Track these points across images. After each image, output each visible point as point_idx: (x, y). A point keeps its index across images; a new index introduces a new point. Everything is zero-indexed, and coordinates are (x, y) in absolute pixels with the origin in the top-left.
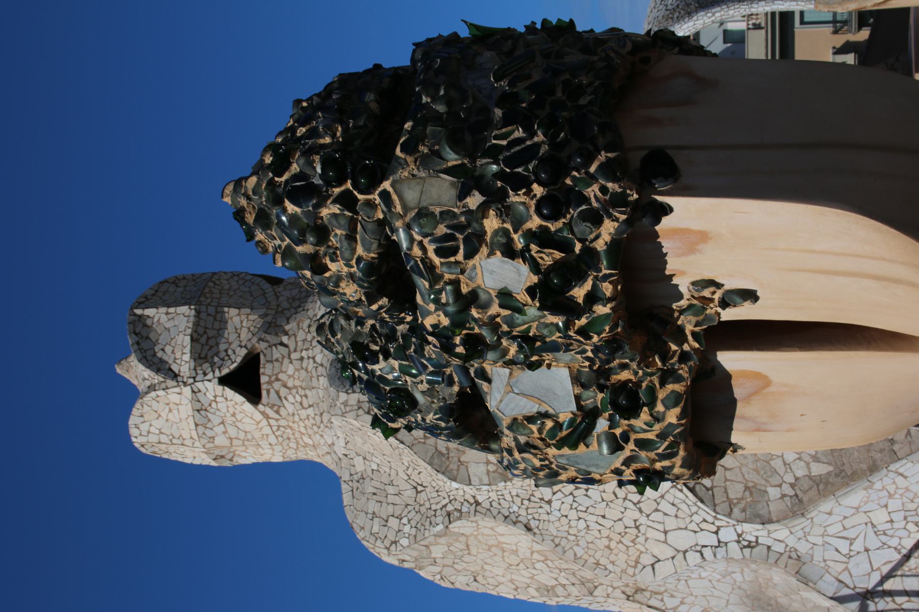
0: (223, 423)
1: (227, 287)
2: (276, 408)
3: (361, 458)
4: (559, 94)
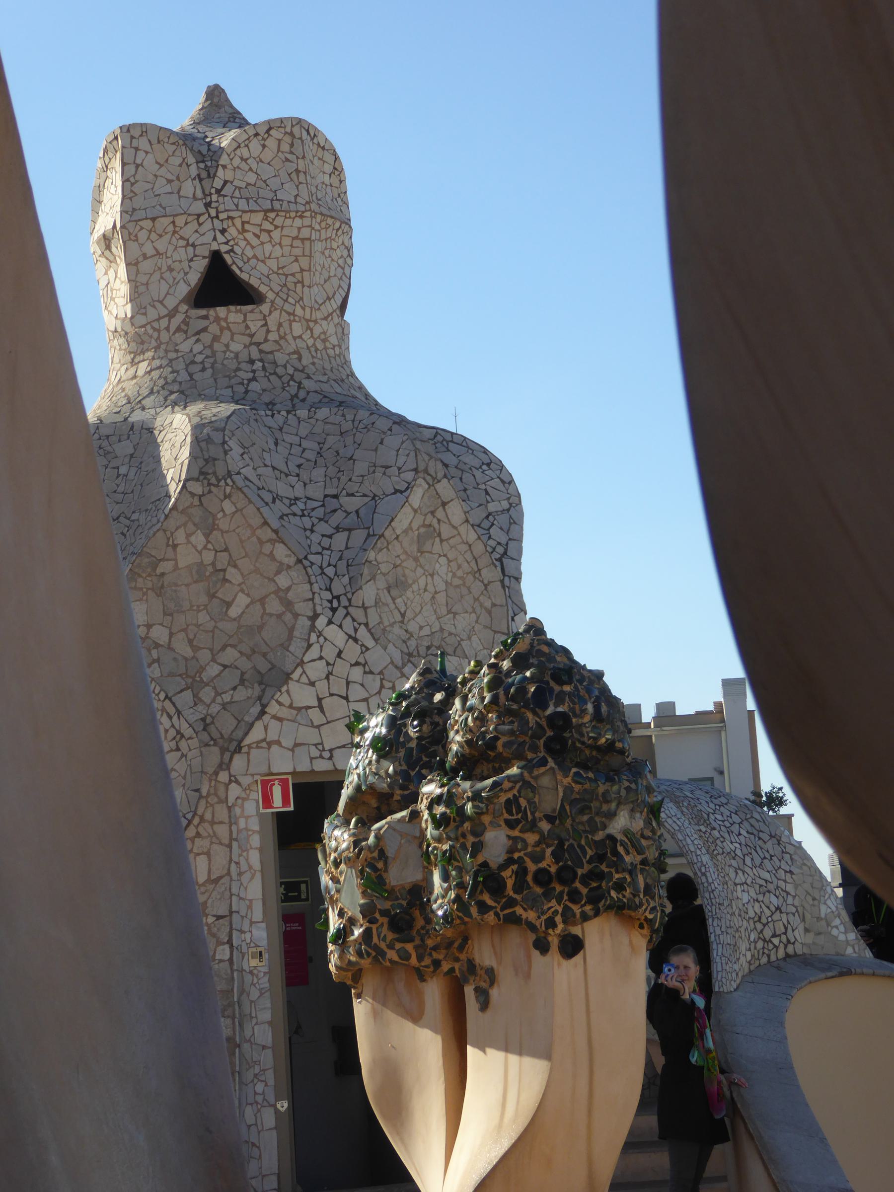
0: (158, 253)
1: (334, 245)
2: (184, 327)
3: (131, 451)
4: (617, 876)
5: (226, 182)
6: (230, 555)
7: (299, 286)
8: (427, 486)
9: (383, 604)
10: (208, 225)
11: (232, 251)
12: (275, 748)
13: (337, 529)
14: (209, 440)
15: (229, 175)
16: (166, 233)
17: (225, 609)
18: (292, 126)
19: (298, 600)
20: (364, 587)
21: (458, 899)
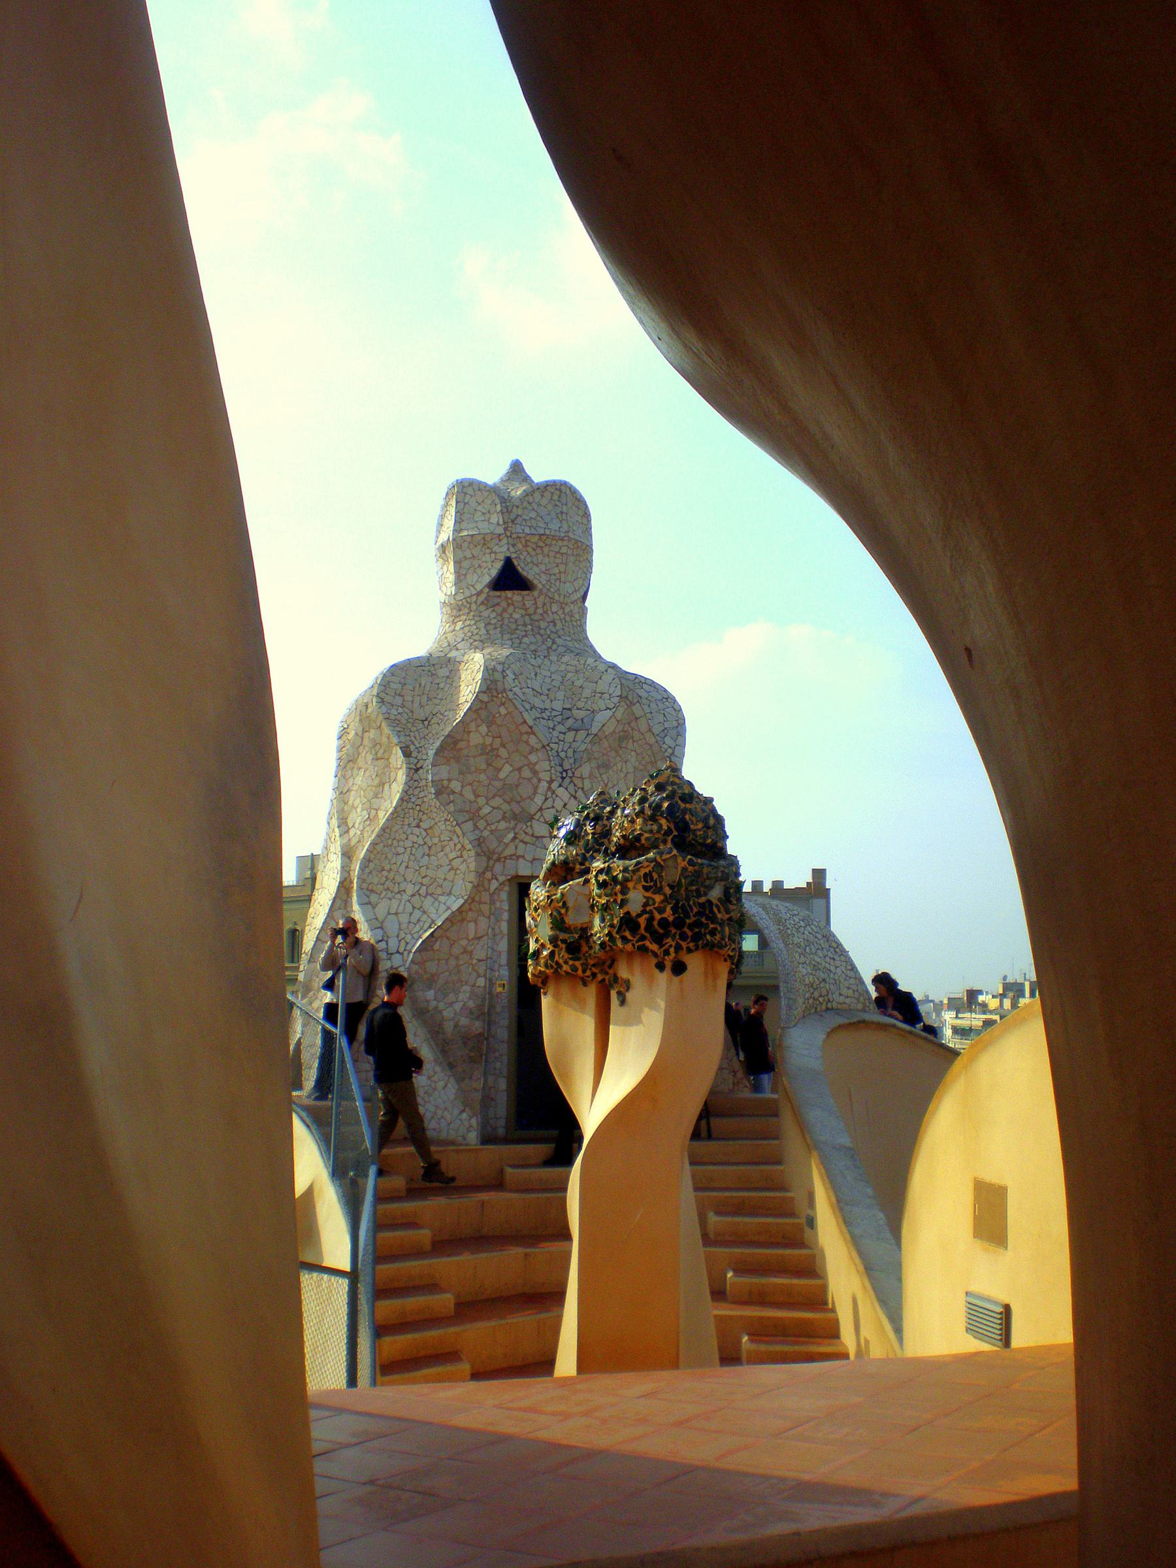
4: (712, 926)
10: (505, 541)
12: (521, 860)
13: (569, 729)
14: (494, 670)
15: (520, 512)
21: (609, 934)
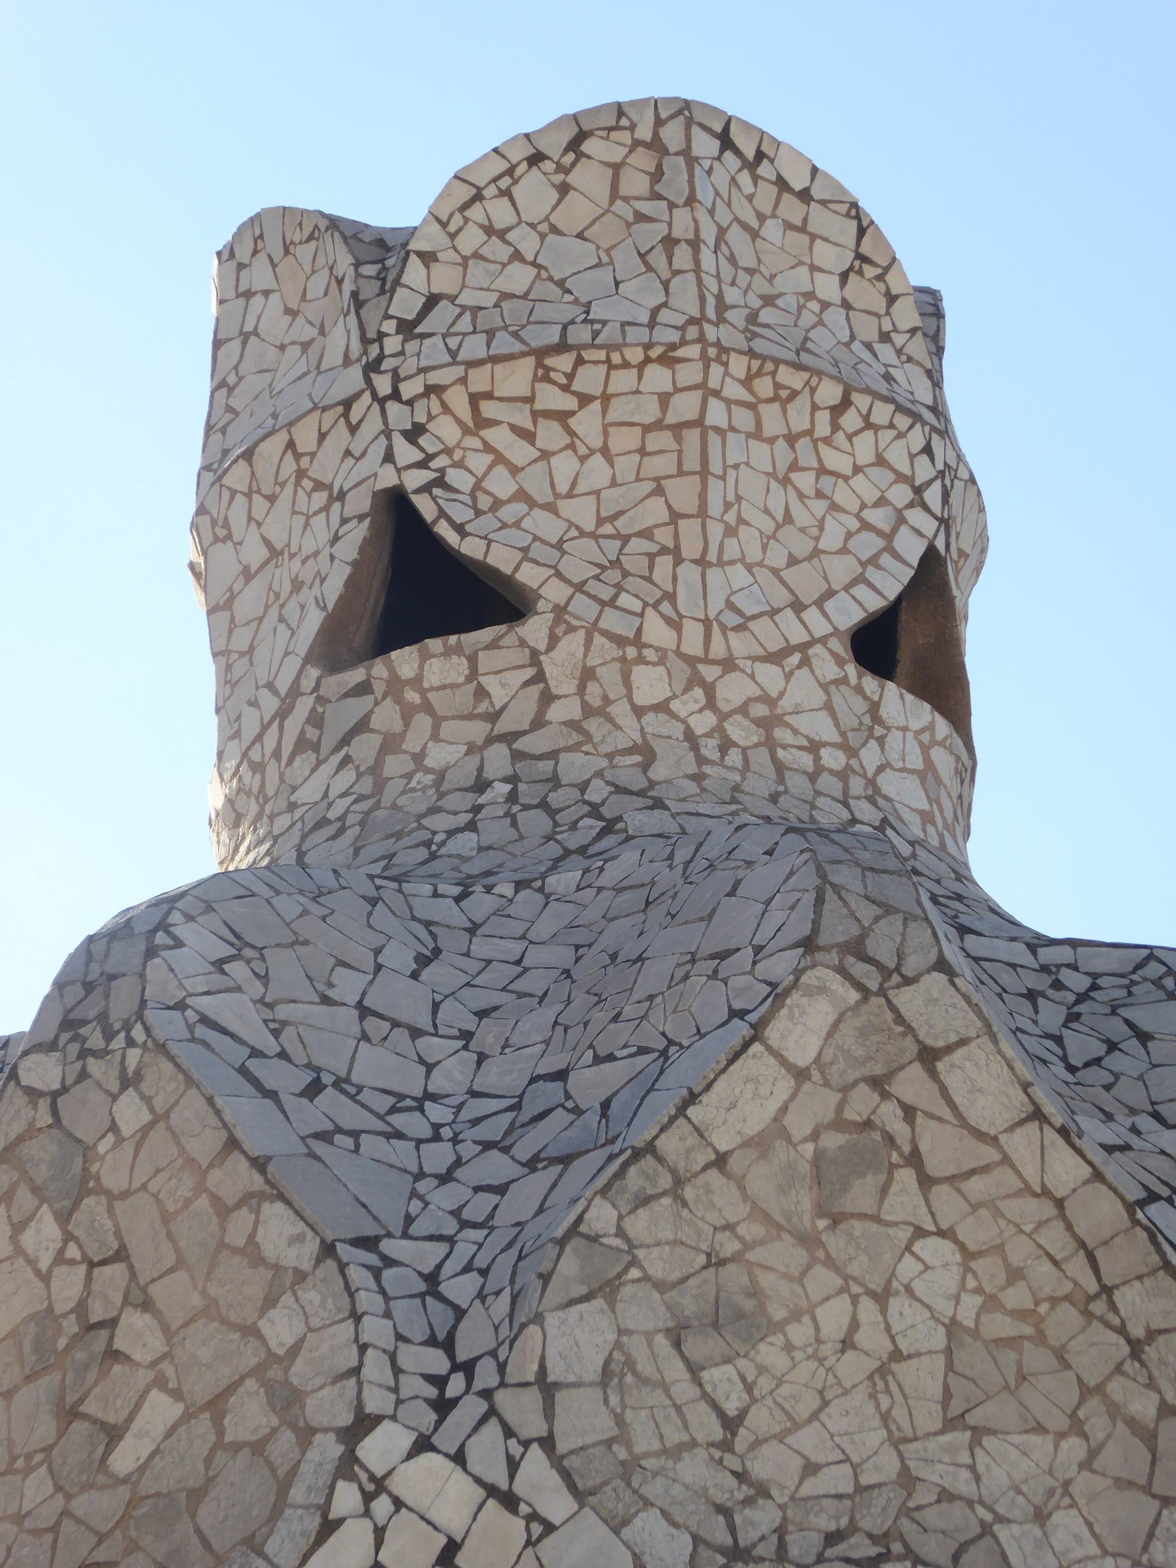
0: (275, 553)
2: (312, 733)
5: (432, 301)
6: (131, 1268)
7: (664, 563)
8: (854, 996)
9: (643, 1380)
11: (440, 482)
15: (444, 279)
16: (282, 485)
17: (101, 1449)
18: (659, 122)
19: (319, 1381)
20: (552, 1320)
